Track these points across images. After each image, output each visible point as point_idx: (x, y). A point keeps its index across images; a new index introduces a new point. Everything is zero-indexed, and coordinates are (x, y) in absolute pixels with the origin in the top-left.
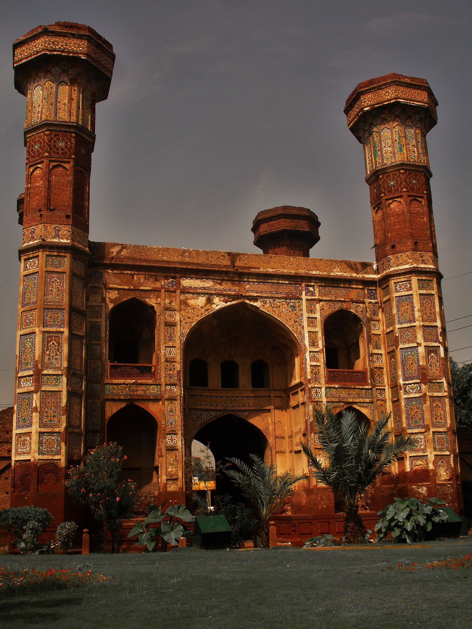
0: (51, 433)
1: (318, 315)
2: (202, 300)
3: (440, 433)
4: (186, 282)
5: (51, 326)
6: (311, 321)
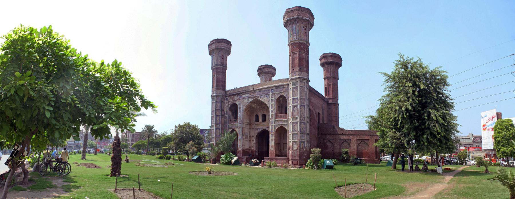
1: (274, 99)
2: (247, 100)
4: (244, 96)
6: (272, 101)
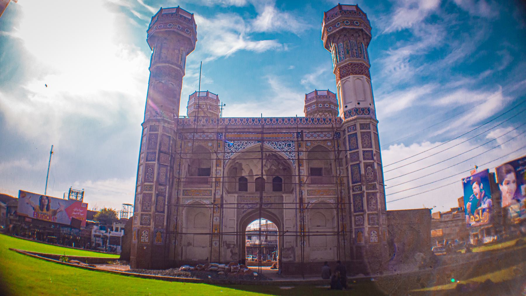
0: (146, 215)
5: (150, 161)
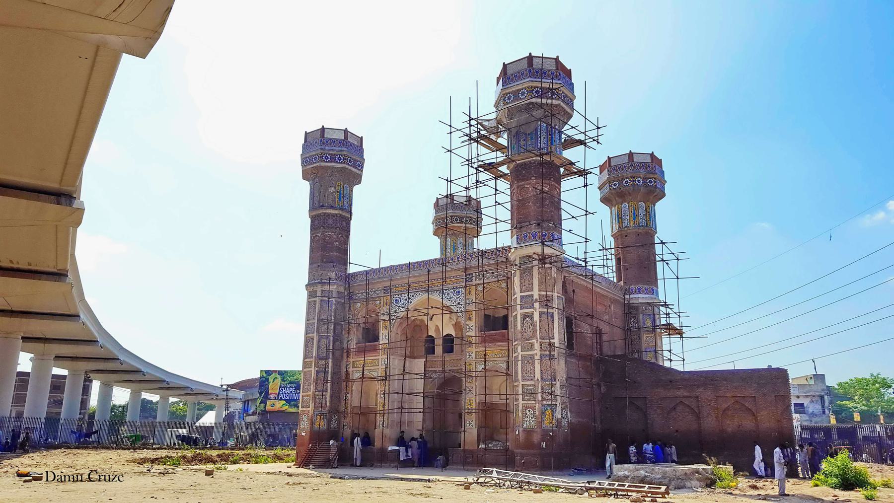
3: (529, 385)
